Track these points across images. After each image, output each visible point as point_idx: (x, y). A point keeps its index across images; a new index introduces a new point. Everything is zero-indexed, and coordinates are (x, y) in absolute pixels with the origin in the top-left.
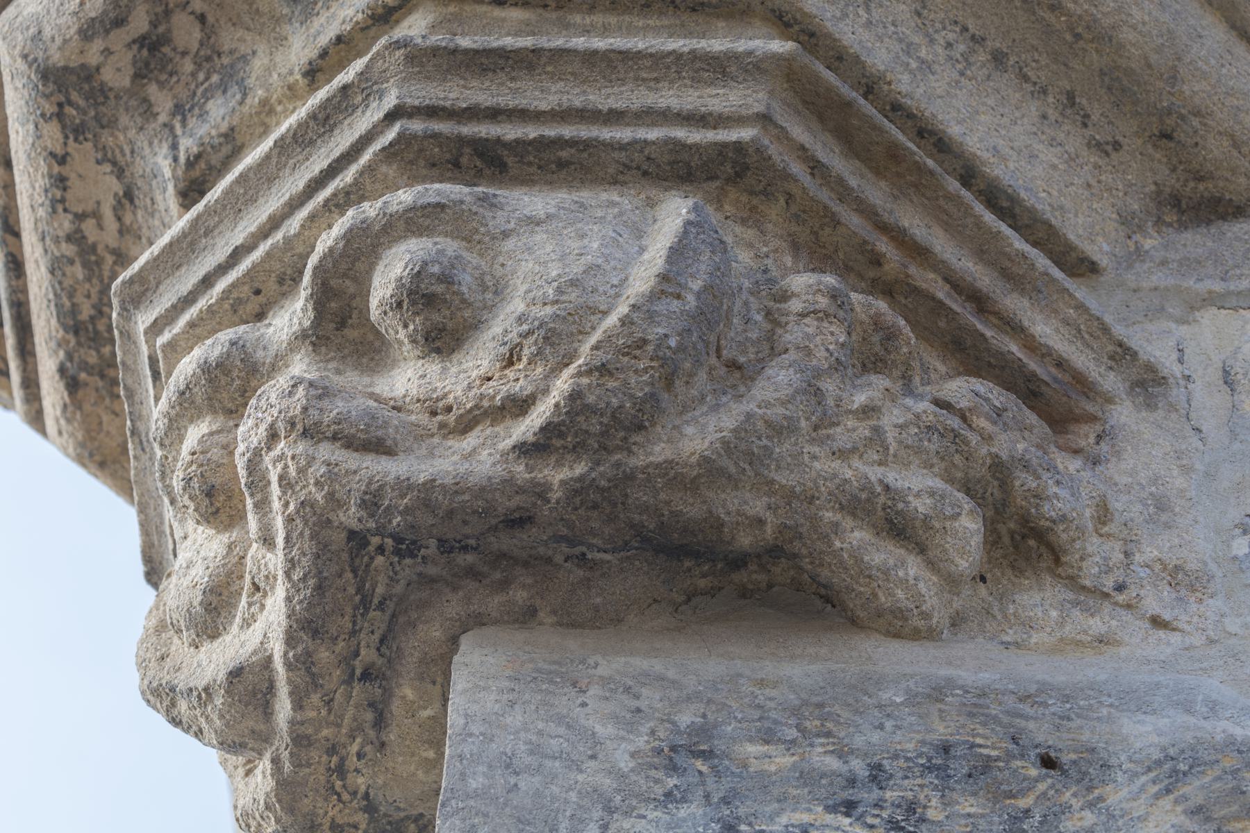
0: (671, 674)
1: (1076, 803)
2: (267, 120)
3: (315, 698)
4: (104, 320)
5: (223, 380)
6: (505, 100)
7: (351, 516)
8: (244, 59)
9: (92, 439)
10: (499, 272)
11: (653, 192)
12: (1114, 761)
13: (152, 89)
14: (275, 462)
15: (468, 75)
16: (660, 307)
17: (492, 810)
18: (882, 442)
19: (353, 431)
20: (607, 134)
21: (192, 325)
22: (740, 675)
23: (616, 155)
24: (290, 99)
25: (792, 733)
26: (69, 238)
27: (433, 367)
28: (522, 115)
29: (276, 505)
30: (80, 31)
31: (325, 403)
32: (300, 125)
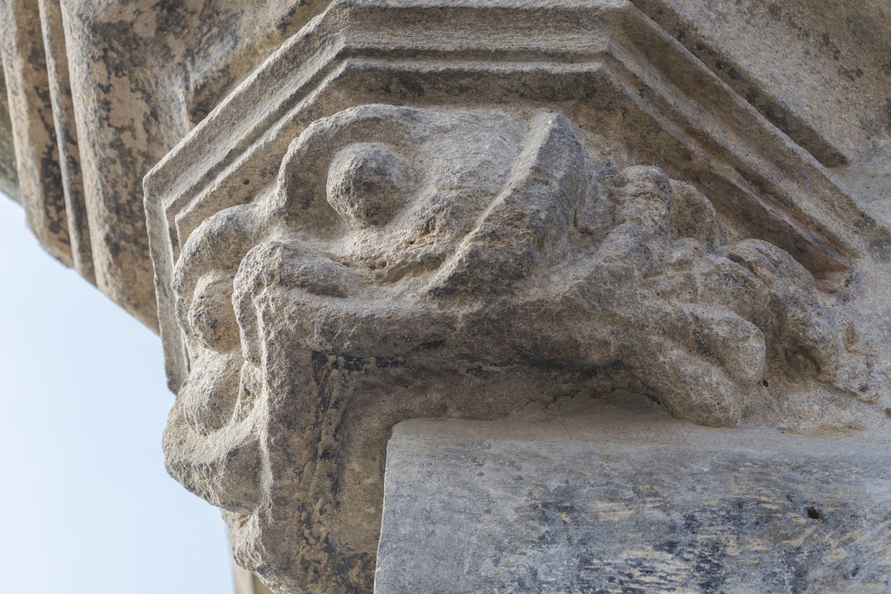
0: (543, 452)
1: (833, 543)
2: (252, 60)
3: (290, 471)
4: (138, 203)
5: (223, 245)
6: (422, 43)
7: (314, 341)
8: (235, 16)
9: (130, 288)
10: (418, 166)
11: (528, 109)
12: (860, 513)
13: (170, 39)
15: (395, 26)
16: (534, 190)
17: (416, 550)
18: (692, 286)
19: (315, 280)
20: (494, 67)
21: (200, 206)
22: (592, 453)
23: (501, 82)
24: (268, 44)
25: (630, 494)
26: (112, 145)
27: (372, 235)
28: (434, 54)
29: (261, 333)
31: (295, 261)
32: (276, 63)
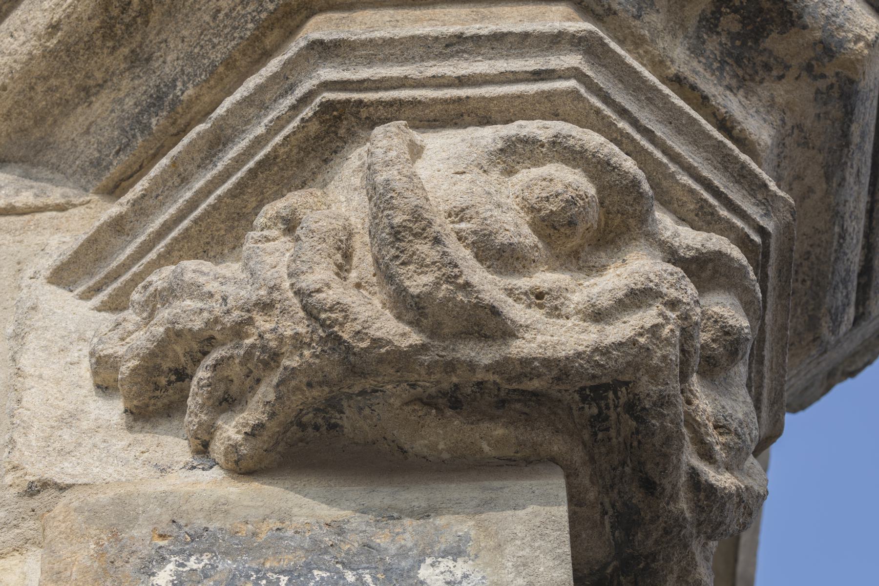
2: (628, 42)
5: (630, 199)
7: (647, 387)
21: (598, 112)
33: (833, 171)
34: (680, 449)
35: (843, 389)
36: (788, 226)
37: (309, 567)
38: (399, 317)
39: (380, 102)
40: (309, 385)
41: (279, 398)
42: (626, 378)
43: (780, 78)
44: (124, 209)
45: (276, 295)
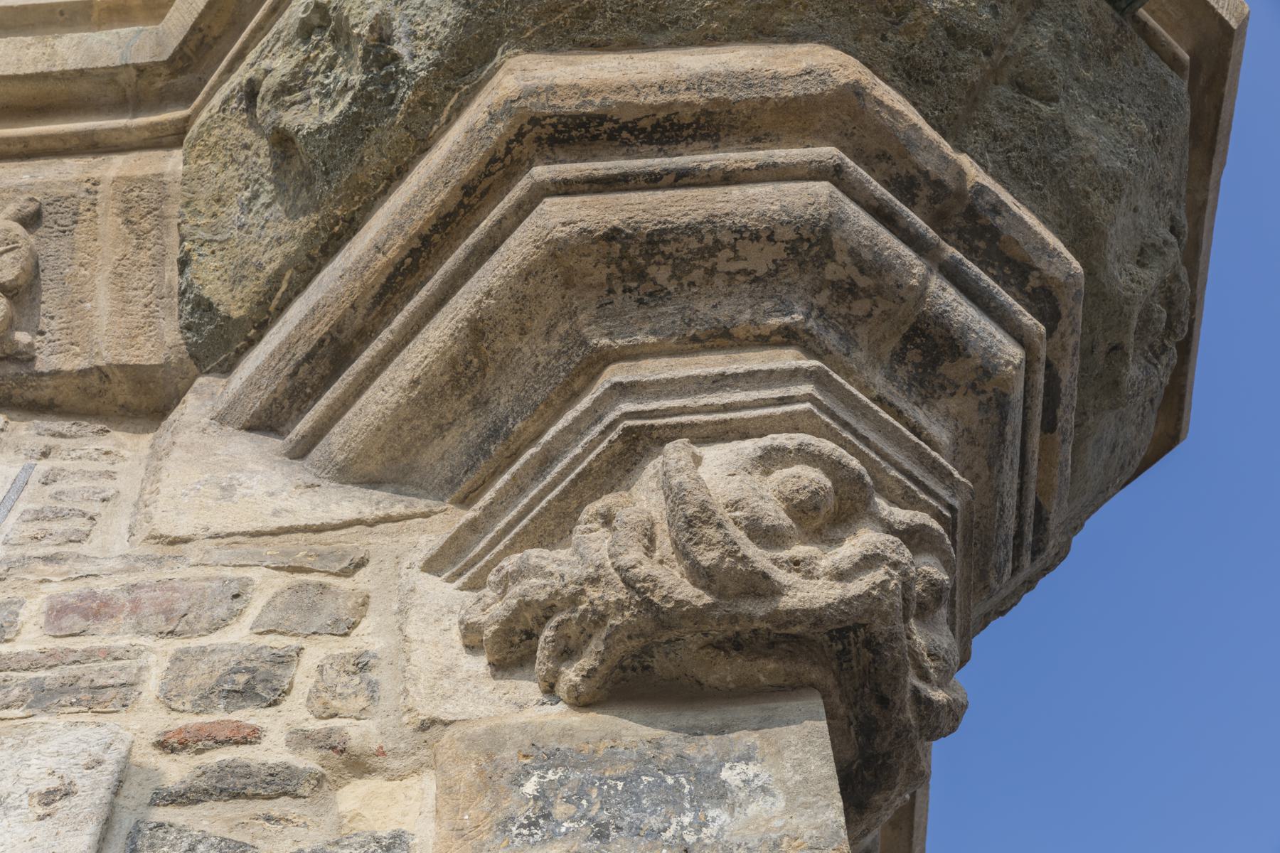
5: (856, 488)
7: (878, 627)
13: (826, 293)
14: (887, 573)
21: (827, 425)
26: (716, 241)
30: (852, 248)
33: (994, 461)
34: (906, 673)
35: (996, 625)
36: (969, 503)
37: (638, 774)
38: (694, 584)
39: (666, 426)
40: (630, 637)
41: (606, 648)
42: (864, 621)
43: (953, 394)
44: (477, 514)
45: (601, 572)
